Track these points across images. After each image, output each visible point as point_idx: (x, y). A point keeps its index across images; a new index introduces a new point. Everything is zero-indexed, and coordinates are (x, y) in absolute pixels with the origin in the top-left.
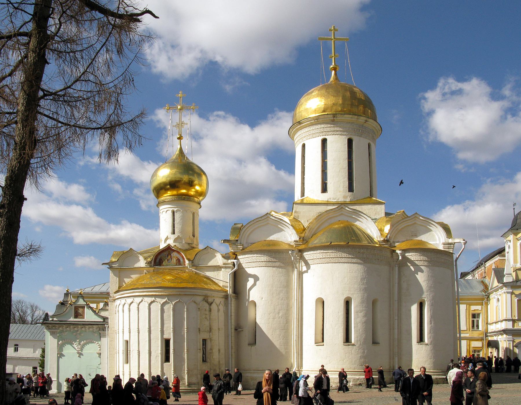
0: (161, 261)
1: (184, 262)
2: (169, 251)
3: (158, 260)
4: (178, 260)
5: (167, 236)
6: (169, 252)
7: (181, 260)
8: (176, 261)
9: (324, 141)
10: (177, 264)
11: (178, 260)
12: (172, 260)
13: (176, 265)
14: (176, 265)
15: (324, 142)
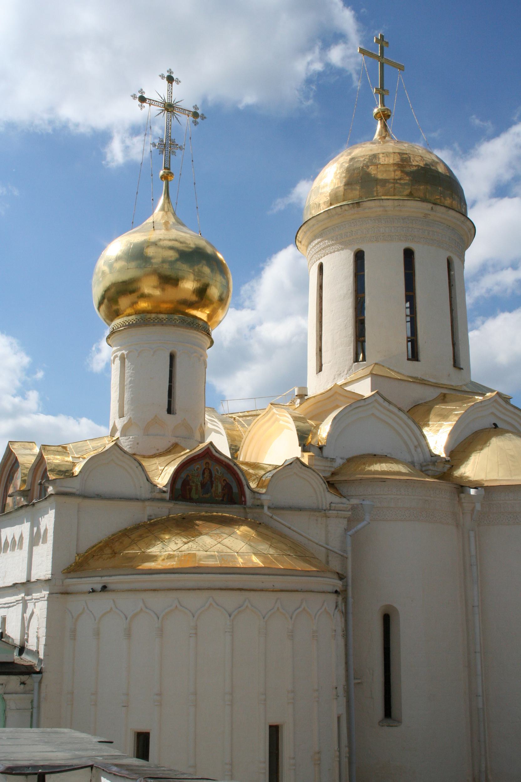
0: (188, 487)
1: (242, 493)
2: (207, 460)
3: (179, 485)
4: (227, 487)
5: (156, 416)
6: (207, 463)
7: (235, 489)
8: (223, 490)
9: (409, 255)
10: (223, 497)
11: (227, 487)
12: (212, 487)
13: (222, 500)
14: (222, 502)
15: (409, 255)
